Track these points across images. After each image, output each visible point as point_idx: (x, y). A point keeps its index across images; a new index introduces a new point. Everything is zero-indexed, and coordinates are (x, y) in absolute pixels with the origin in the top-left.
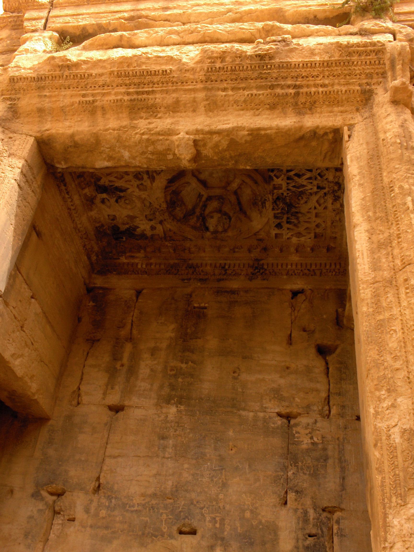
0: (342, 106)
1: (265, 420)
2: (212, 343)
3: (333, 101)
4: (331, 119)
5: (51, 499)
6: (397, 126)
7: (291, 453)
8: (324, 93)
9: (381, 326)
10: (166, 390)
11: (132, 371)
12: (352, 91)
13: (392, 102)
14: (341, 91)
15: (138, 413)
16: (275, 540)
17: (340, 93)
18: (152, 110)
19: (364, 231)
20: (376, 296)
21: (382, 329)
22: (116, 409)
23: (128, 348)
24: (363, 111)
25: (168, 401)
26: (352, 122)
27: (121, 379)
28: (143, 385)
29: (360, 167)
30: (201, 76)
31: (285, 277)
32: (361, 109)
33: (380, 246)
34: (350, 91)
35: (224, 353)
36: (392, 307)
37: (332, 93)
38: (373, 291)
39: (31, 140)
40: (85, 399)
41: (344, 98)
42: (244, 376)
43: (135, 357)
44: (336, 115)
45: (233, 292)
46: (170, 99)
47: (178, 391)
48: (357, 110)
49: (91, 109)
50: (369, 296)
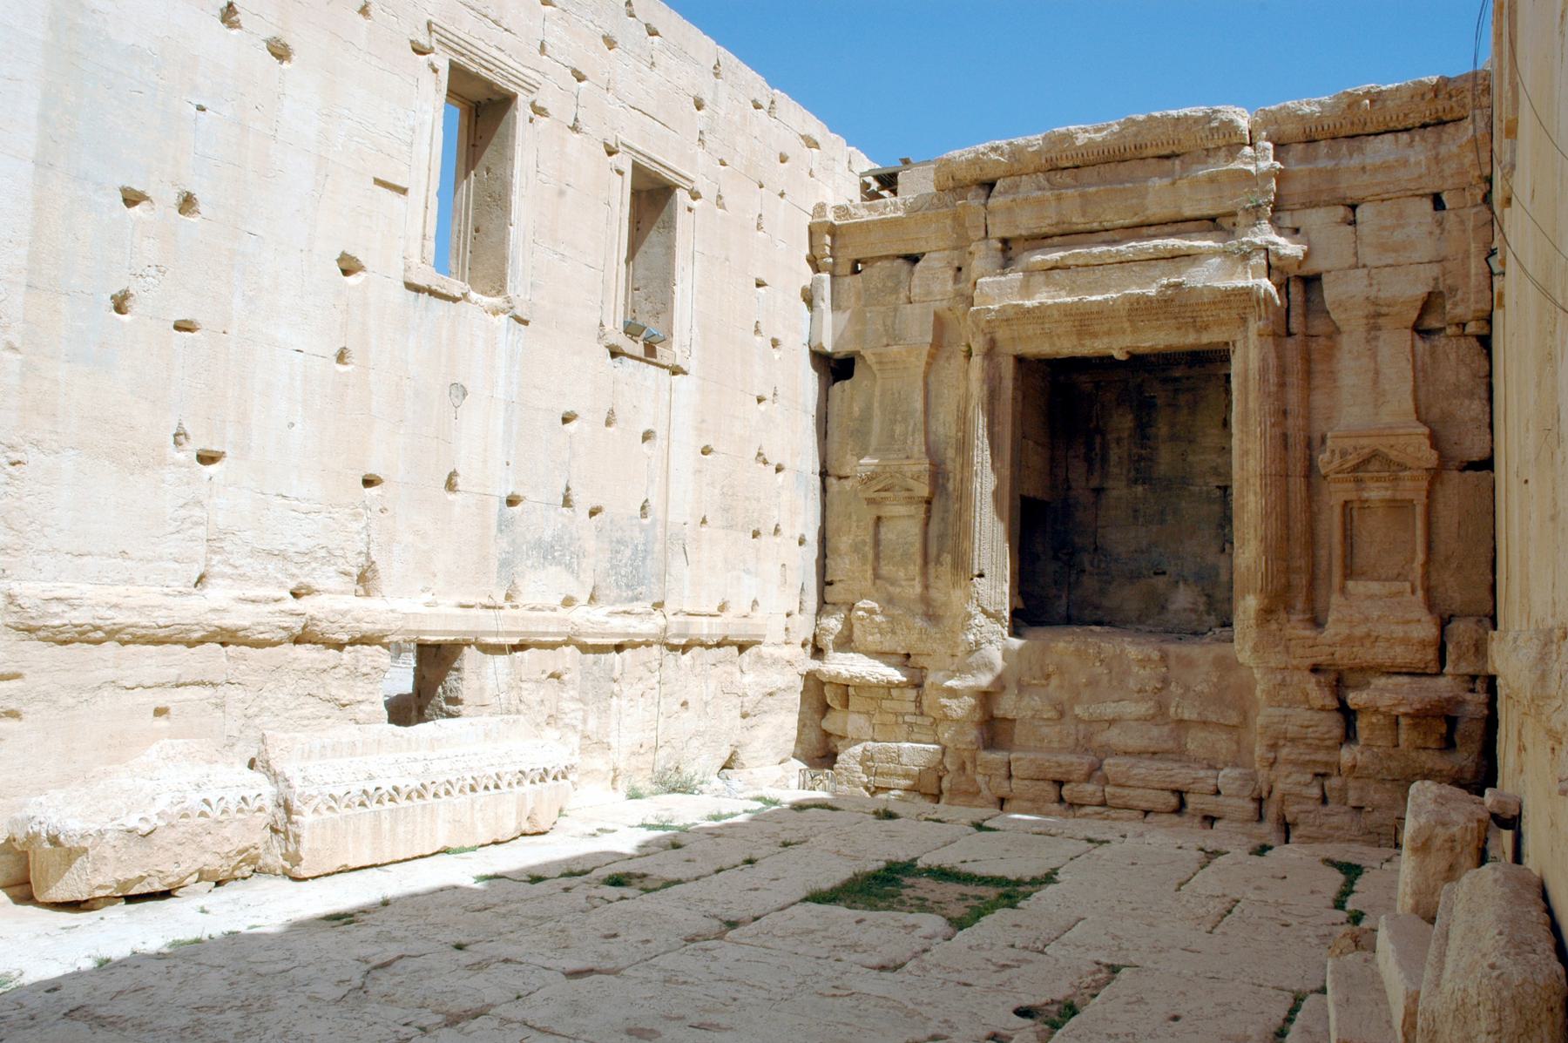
1: (1208, 492)
2: (1163, 429)
3: (1221, 323)
5: (1065, 558)
10: (1133, 473)
11: (1104, 459)
15: (1114, 493)
16: (1218, 575)
18: (1094, 335)
22: (1099, 491)
23: (1098, 440)
25: (1136, 482)
27: (1097, 466)
28: (1114, 470)
30: (1123, 313)
33: (1246, 453)
35: (1173, 438)
39: (1011, 360)
40: (1074, 485)
42: (1190, 458)
43: (1105, 447)
45: (1176, 380)
46: (1106, 328)
47: (1141, 472)
49: (1049, 335)
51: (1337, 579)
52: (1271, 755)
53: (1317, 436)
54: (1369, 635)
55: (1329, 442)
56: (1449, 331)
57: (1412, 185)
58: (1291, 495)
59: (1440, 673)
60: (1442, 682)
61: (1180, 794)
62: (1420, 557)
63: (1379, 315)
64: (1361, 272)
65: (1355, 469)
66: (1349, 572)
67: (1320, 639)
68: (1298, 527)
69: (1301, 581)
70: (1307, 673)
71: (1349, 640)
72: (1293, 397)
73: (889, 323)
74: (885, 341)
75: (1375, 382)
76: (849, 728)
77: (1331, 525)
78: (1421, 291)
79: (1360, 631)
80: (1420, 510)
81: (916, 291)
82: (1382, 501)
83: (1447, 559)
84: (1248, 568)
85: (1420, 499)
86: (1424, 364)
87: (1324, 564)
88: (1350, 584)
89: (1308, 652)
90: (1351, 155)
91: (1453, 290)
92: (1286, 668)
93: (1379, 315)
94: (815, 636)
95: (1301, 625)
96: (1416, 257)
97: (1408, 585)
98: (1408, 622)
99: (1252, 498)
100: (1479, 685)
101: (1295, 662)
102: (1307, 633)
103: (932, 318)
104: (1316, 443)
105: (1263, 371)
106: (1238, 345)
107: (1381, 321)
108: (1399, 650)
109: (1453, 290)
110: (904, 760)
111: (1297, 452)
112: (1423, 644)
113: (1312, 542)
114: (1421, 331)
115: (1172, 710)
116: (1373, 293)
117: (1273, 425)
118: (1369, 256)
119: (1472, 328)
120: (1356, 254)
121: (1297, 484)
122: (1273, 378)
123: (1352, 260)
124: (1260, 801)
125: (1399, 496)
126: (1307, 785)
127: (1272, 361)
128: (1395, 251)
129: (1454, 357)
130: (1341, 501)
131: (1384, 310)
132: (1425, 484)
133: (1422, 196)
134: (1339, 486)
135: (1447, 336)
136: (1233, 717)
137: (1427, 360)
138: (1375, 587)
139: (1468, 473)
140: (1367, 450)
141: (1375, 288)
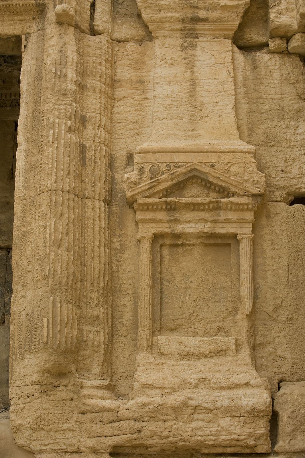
0: (21, 15)
4: (11, 27)
6: (57, 52)
7: (8, 282)
8: (5, 6)
9: (24, 236)
12: (28, 5)
13: (57, 23)
14: (19, 5)
17: (18, 6)
19: (23, 151)
20: (24, 211)
21: (24, 239)
24: (38, 20)
26: (28, 31)
29: (28, 83)
31: (9, 108)
32: (37, 18)
33: (32, 167)
34: (26, 5)
36: (31, 223)
37: (11, 6)
38: (23, 206)
41: (22, 9)
44: (16, 23)
48: (34, 19)
50: (20, 210)
51: (143, 334)
53: (121, 155)
54: (185, 405)
55: (137, 158)
56: (272, 45)
58: (89, 223)
62: (247, 306)
65: (168, 192)
66: (158, 326)
67: (123, 412)
68: (96, 266)
69: (96, 334)
71: (158, 413)
72: (93, 103)
75: (192, 94)
77: (136, 264)
79: (174, 399)
80: (245, 248)
82: (200, 236)
83: (277, 308)
84: (30, 317)
85: (245, 232)
86: (245, 79)
87: (127, 316)
88: (162, 340)
89: (107, 429)
93: (196, 20)
95: (99, 393)
97: (231, 340)
98: (234, 387)
101: (91, 443)
104: (120, 162)
105: (62, 63)
106: (33, 39)
107: (199, 26)
108: (225, 422)
111: (100, 169)
112: (254, 414)
113: (111, 290)
117: (69, 130)
121: (95, 210)
122: (71, 74)
125: (222, 229)
127: (72, 55)
130: (150, 234)
131: (202, 14)
132: (250, 216)
134: (150, 216)
137: (249, 74)
138: (192, 343)
139: (296, 206)
140: (182, 170)
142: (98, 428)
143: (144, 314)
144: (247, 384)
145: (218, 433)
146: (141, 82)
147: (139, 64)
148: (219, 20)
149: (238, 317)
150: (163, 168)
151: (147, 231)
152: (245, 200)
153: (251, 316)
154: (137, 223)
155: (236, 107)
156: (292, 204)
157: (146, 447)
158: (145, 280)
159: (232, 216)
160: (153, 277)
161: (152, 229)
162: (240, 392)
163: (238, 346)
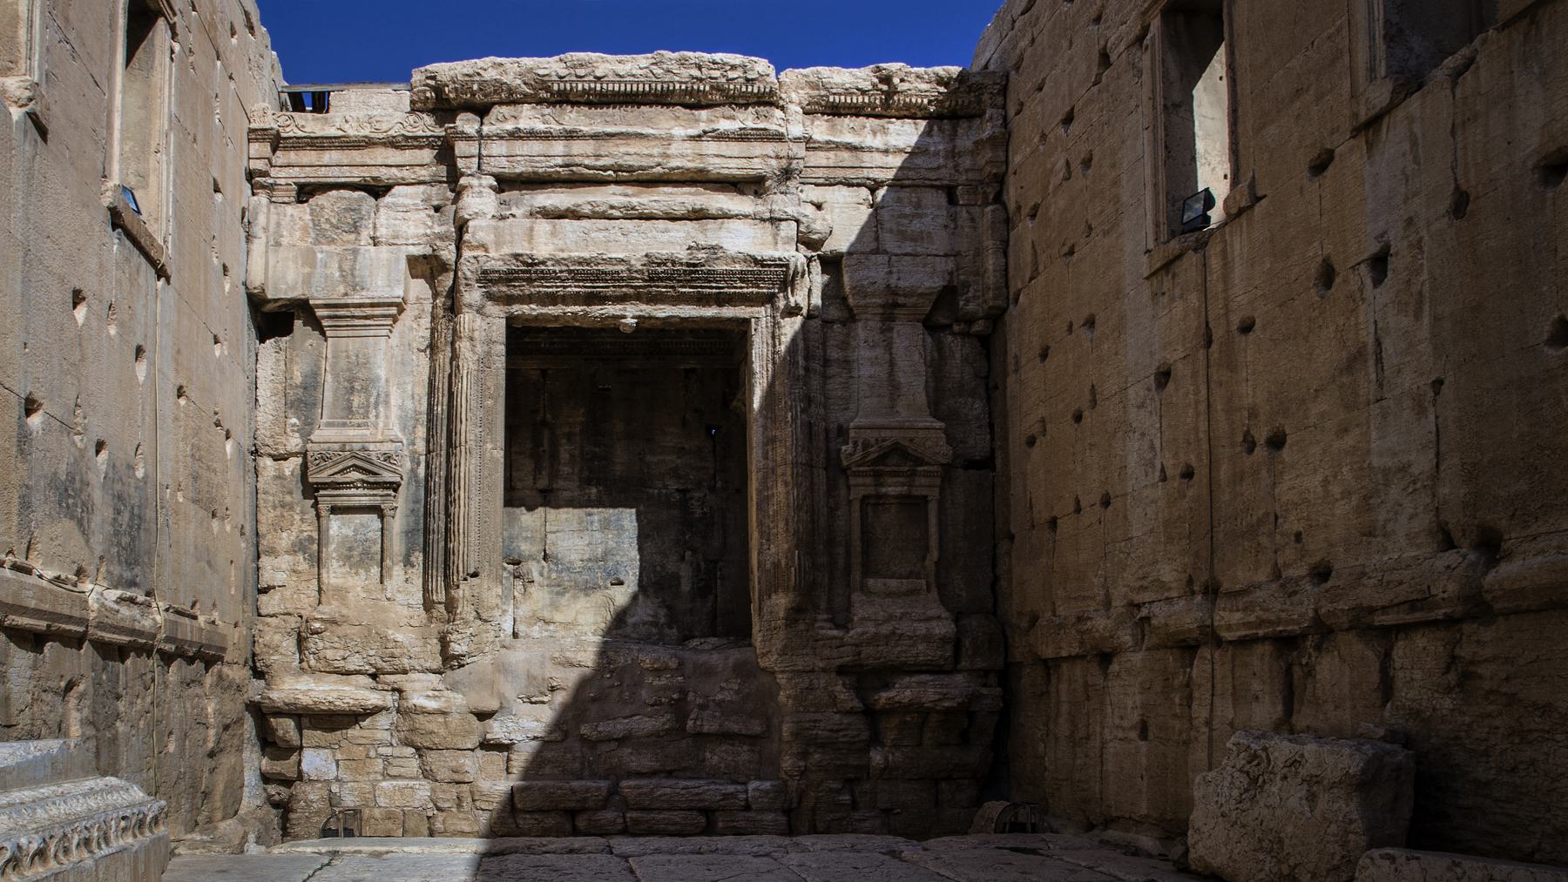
33: (770, 441)
52: (802, 763)
53: (833, 426)
54: (893, 633)
55: (852, 434)
56: (956, 328)
57: (932, 175)
59: (954, 671)
60: (959, 678)
61: (707, 812)
63: (896, 305)
64: (881, 259)
65: (875, 462)
70: (833, 675)
72: (815, 382)
73: (347, 267)
74: (341, 289)
75: (891, 374)
76: (304, 767)
78: (937, 283)
79: (885, 629)
81: (382, 232)
85: (933, 494)
87: (841, 562)
88: (871, 582)
89: (835, 653)
90: (874, 133)
91: (966, 285)
92: (813, 671)
93: (896, 305)
94: (254, 655)
95: (828, 625)
96: (933, 249)
99: (781, 488)
100: (992, 679)
102: (835, 633)
103: (403, 265)
109: (966, 285)
110: (382, 801)
112: (944, 640)
114: (930, 326)
115: (690, 723)
116: (893, 282)
118: (890, 243)
119: (978, 327)
120: (877, 239)
123: (874, 245)
124: (787, 812)
125: (917, 492)
126: (838, 791)
128: (914, 240)
129: (958, 349)
131: (901, 300)
132: (938, 481)
133: (938, 188)
134: (860, 480)
135: (954, 334)
136: (756, 727)
138: (893, 583)
141: (895, 276)
142: (827, 652)
143: (857, 560)
144: (939, 617)
145: (917, 656)
146: (847, 362)
147: (845, 345)
148: (915, 305)
149: (927, 563)
150: (873, 441)
151: (857, 494)
152: (935, 468)
153: (937, 564)
154: (849, 487)
155: (926, 387)
156: (966, 468)
157: (861, 666)
158: (856, 534)
159: (923, 480)
160: (863, 533)
161: (862, 492)
162: (934, 623)
163: (928, 585)
